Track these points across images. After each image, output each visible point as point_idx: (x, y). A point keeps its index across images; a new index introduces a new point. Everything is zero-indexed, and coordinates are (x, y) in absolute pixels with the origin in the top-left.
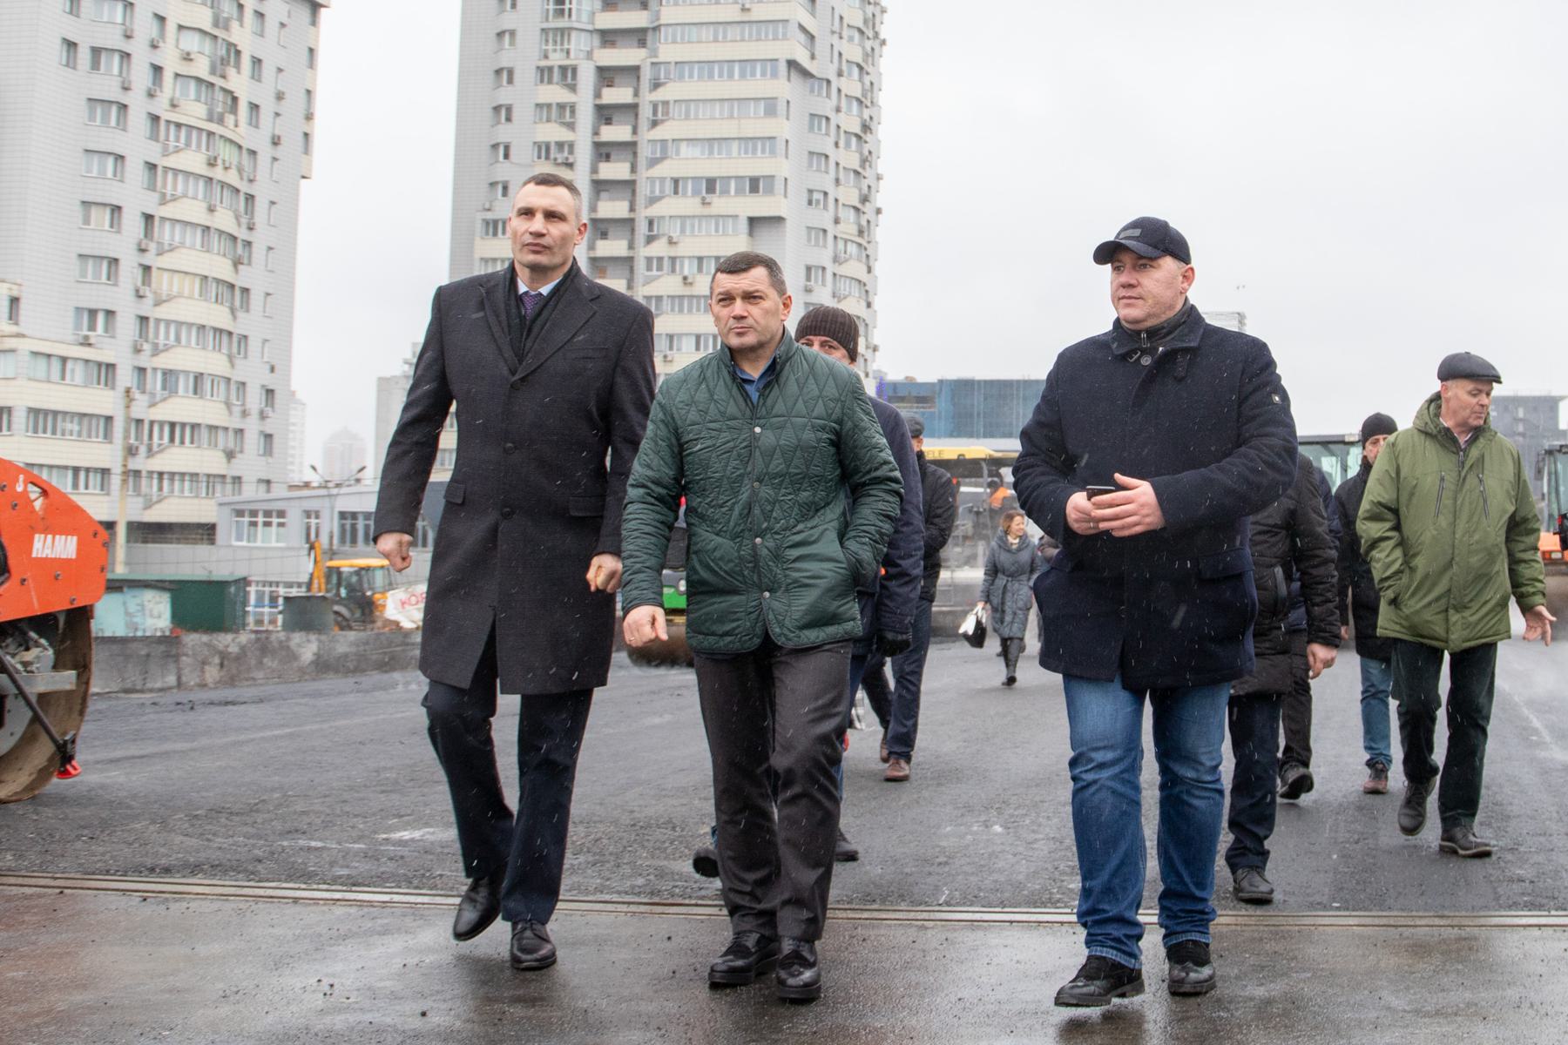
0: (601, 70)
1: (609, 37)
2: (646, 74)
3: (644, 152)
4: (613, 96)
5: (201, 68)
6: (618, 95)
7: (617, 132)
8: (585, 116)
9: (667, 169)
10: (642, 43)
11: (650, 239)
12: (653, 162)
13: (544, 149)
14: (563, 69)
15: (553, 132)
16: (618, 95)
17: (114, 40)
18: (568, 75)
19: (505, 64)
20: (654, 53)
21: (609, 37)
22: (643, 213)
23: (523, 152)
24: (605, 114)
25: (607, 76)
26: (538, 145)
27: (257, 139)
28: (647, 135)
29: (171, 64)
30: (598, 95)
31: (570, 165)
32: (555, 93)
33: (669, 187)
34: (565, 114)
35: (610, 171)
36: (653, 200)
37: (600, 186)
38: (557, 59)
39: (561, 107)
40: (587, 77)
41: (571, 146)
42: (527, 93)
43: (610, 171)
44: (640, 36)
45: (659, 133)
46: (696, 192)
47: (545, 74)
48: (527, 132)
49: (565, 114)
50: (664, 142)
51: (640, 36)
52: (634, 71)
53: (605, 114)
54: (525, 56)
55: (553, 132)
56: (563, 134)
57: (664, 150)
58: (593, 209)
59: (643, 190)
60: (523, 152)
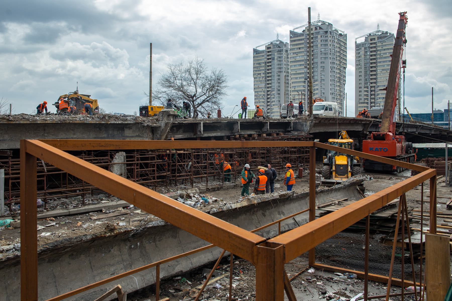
0: (371, 86)
1: (371, 83)
2: (376, 87)
3: (376, 95)
4: (372, 89)
5: (339, 93)
6: (373, 89)
7: (373, 93)
8: (369, 91)
9: (379, 96)
10: (375, 83)
11: (377, 104)
12: (377, 96)
13: (365, 95)
14: (367, 87)
15: (366, 93)
16: (373, 89)
17: (334, 92)
18: (367, 87)
19: (360, 86)
20: (377, 84)
21: (371, 83)
22: (376, 101)
23: (363, 95)
24: (371, 91)
25: (371, 87)
26: (364, 95)
27: (342, 98)
28: (376, 93)
29: (337, 93)
30: (371, 89)
31: (368, 97)
32: (366, 89)
33: (379, 98)
34: (367, 91)
35: (372, 97)
36: (377, 100)
37: (371, 98)
38: (366, 86)
39: (367, 91)
40: (369, 87)
41: (368, 94)
42: (363, 89)
43: (372, 97)
44: (375, 83)
45: (378, 93)
46: (382, 99)
47: (365, 87)
48: (363, 93)
49: (367, 91)
50: (378, 94)
51: (375, 83)
52: (375, 86)
53: (371, 91)
54: (363, 85)
55: (366, 93)
56: (367, 93)
57: (378, 95)
58: (370, 101)
59: (376, 99)
60: (363, 95)
